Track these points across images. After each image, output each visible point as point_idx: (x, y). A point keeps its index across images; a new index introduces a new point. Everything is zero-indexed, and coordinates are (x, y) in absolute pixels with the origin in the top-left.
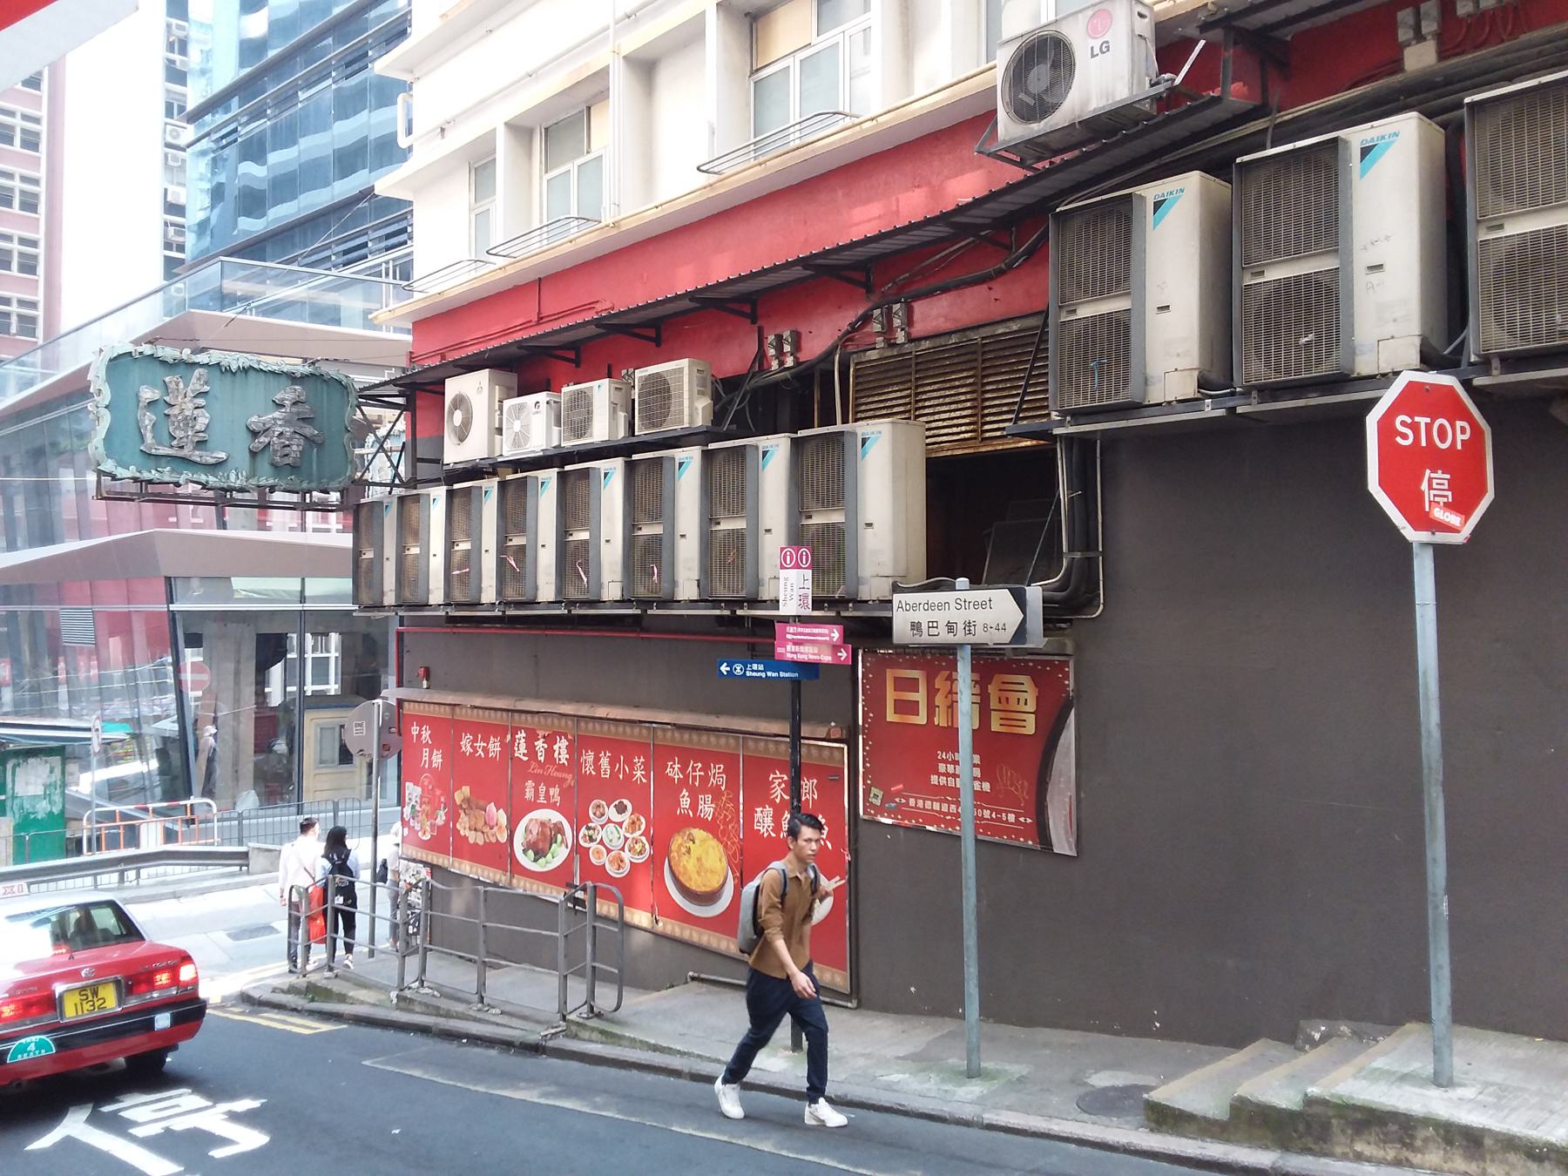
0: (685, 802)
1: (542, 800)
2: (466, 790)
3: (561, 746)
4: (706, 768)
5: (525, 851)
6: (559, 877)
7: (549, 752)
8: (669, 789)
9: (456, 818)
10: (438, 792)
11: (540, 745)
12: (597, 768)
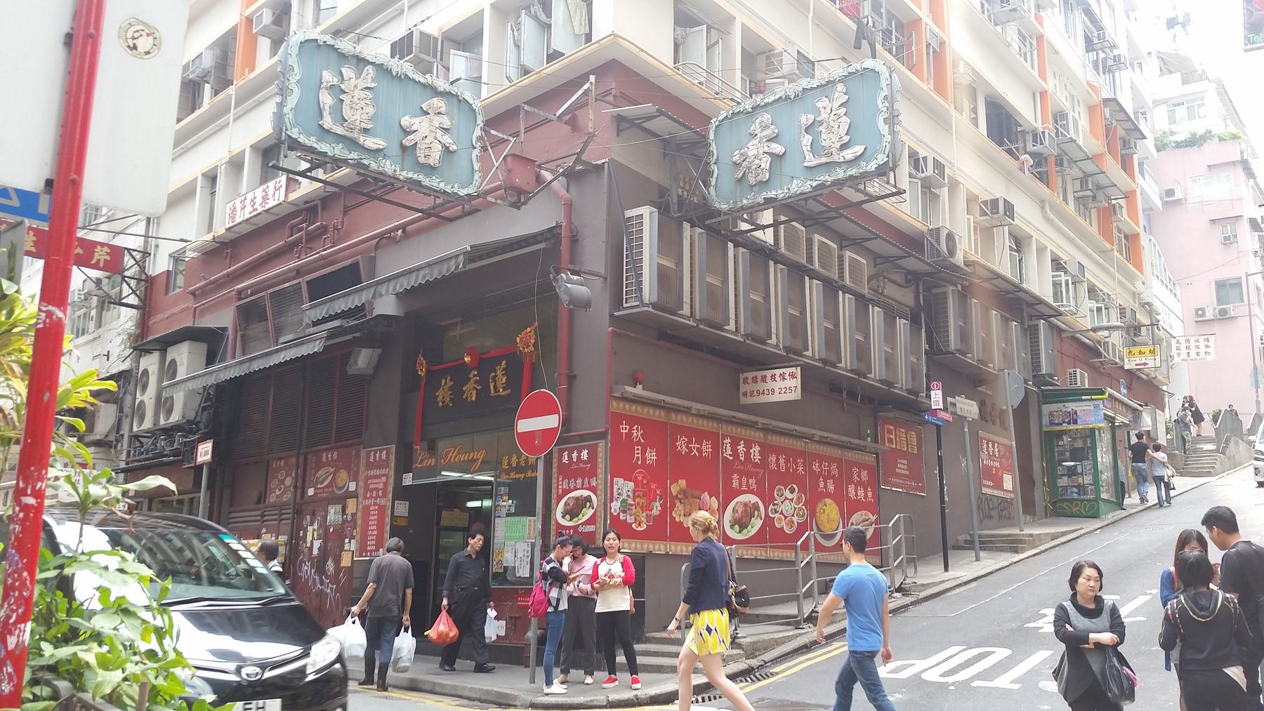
0: (822, 485)
1: (744, 488)
2: (682, 483)
3: (755, 450)
4: (829, 466)
5: (732, 527)
6: (757, 539)
7: (747, 454)
8: (815, 477)
9: (673, 506)
10: (653, 486)
11: (741, 448)
12: (778, 466)
